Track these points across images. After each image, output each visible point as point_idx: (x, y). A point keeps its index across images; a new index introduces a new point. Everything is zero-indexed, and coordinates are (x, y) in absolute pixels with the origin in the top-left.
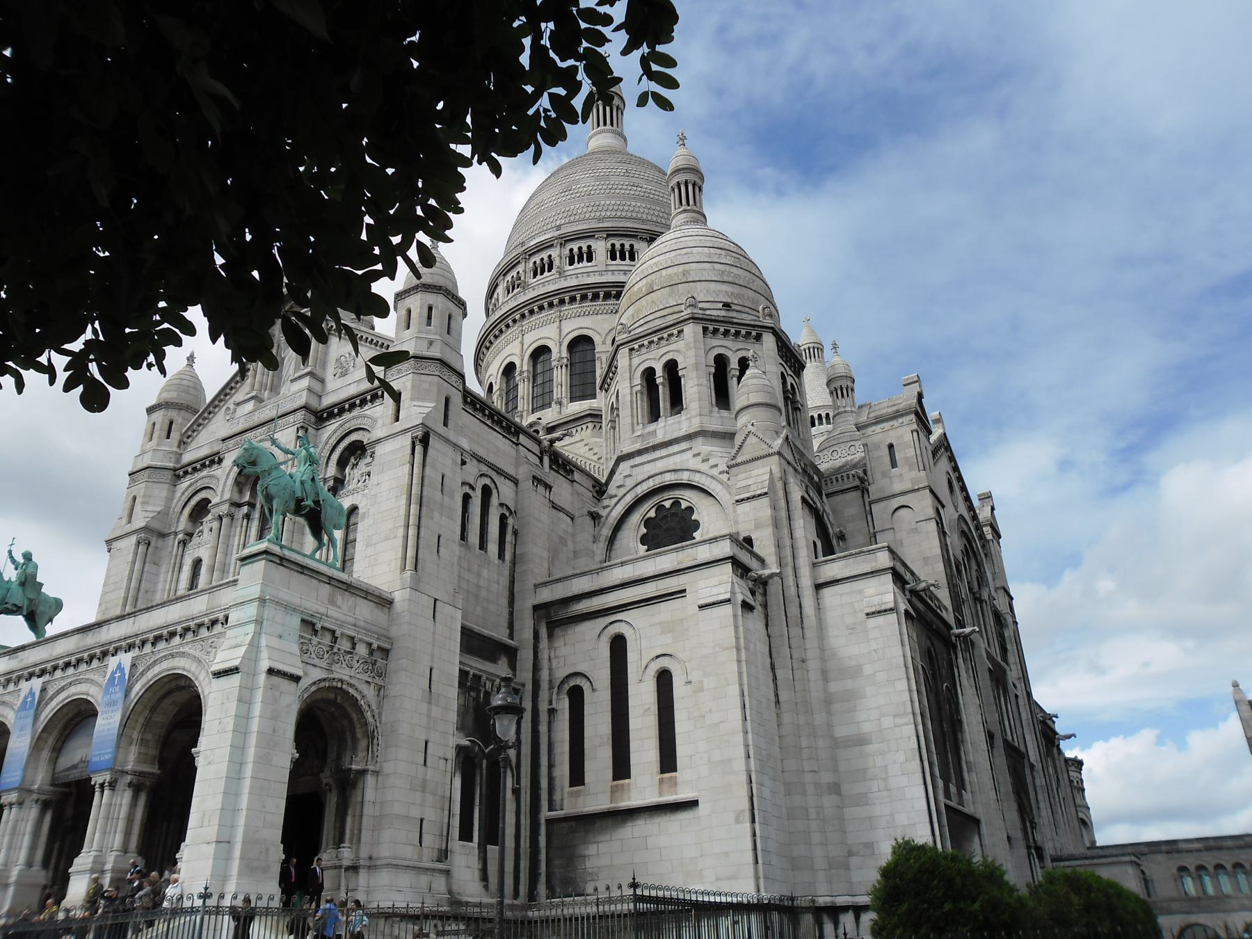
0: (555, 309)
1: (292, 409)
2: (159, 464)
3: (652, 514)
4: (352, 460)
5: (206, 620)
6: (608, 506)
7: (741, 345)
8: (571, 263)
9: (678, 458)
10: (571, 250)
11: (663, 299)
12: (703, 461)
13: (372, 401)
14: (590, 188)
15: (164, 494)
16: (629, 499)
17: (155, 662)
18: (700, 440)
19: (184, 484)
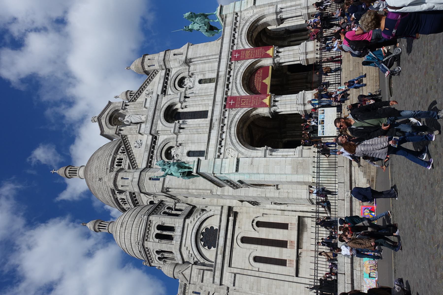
1: (156, 99)
5: (234, 21)
10: (120, 152)
13: (169, 76)
17: (241, 40)
19: (154, 162)
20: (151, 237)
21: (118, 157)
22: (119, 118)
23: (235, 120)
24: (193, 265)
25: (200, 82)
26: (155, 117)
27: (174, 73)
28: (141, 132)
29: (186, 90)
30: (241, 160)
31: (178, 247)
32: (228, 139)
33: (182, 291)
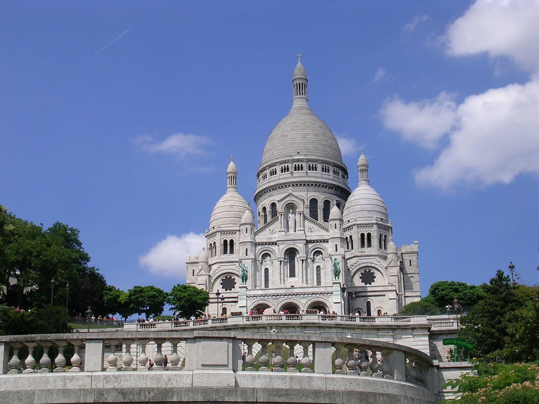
0: (306, 187)
1: (302, 239)
2: (253, 241)
3: (363, 272)
4: (316, 254)
6: (352, 268)
7: (385, 232)
8: (310, 170)
9: (371, 260)
10: (310, 165)
11: (366, 214)
12: (378, 262)
14: (313, 139)
15: (254, 249)
16: (358, 267)
18: (377, 257)
19: (259, 248)
20: (224, 237)
21: (304, 164)
22: (291, 210)
23: (267, 302)
24: (208, 275)
25: (318, 267)
26: (288, 242)
27: (325, 246)
28: (279, 232)
29: (311, 258)
30: (245, 308)
31: (219, 261)
32: (256, 300)
33: (193, 261)
